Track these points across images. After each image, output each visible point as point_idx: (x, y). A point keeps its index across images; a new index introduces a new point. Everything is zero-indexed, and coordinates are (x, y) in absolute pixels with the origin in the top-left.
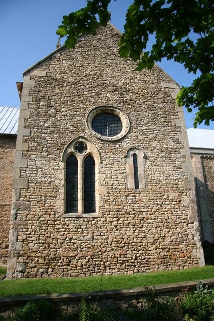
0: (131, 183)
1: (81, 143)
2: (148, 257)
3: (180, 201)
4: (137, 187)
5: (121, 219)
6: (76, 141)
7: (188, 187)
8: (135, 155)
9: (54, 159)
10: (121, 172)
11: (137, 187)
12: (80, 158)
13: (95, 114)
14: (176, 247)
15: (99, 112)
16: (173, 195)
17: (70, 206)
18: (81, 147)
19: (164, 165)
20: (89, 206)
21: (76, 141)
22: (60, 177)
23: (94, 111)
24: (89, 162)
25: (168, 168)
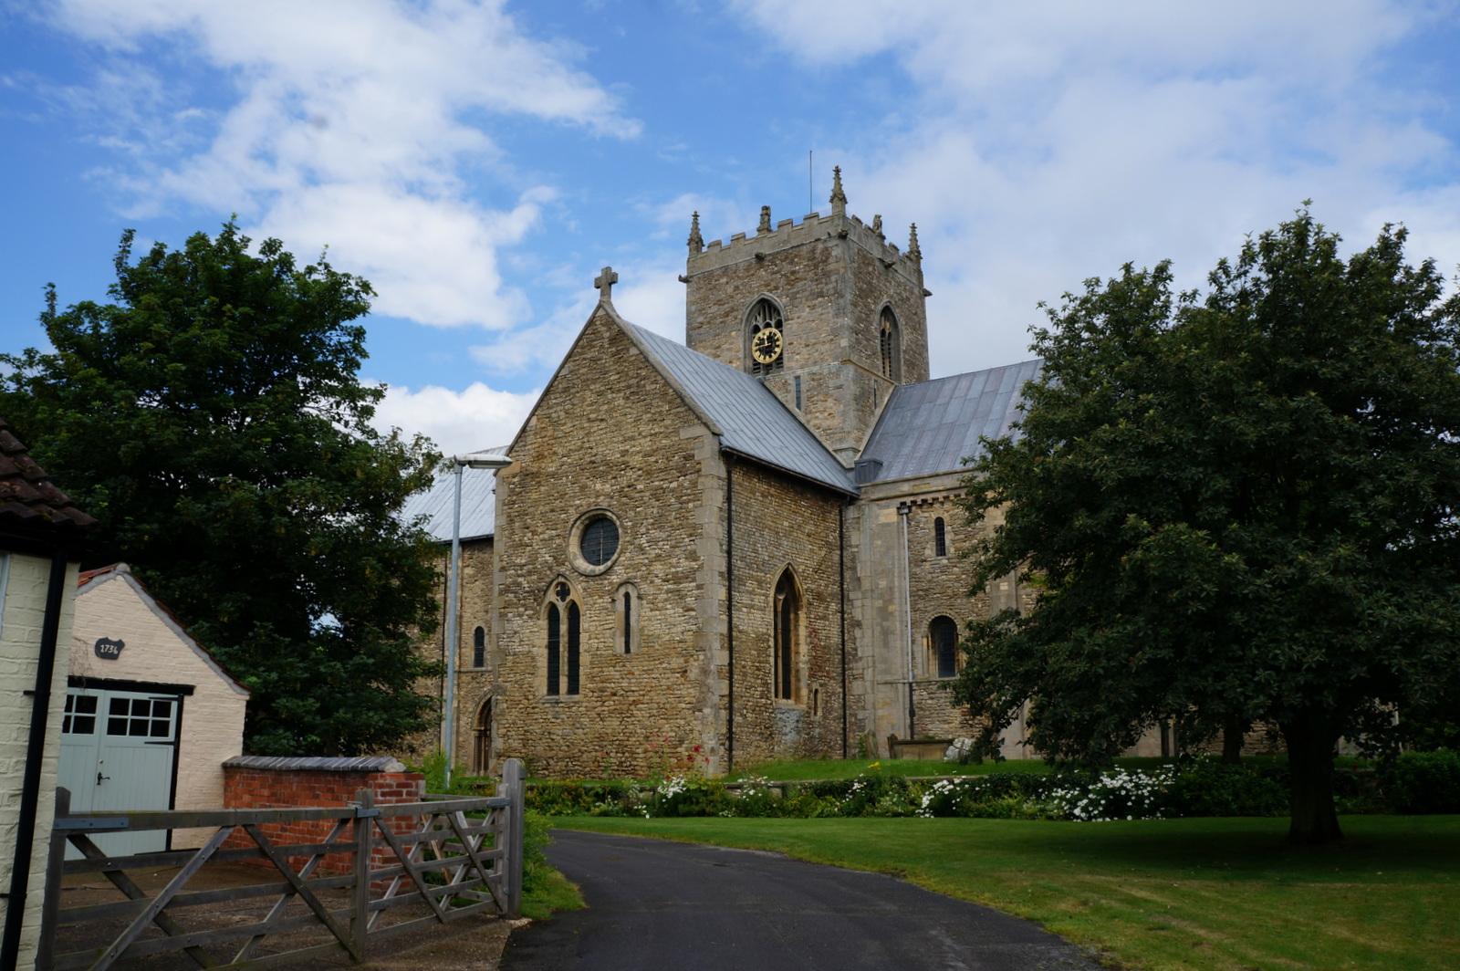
0: (620, 648)
1: (563, 585)
2: (635, 763)
3: (686, 671)
4: (628, 650)
5: (606, 704)
6: (555, 583)
7: (701, 644)
8: (627, 596)
9: (530, 617)
10: (607, 627)
11: (628, 650)
12: (561, 606)
13: (581, 527)
14: (673, 751)
15: (587, 522)
16: (677, 662)
17: (553, 688)
18: (564, 592)
19: (669, 606)
20: (574, 688)
21: (555, 583)
22: (542, 638)
23: (579, 522)
24: (574, 611)
25: (673, 612)
